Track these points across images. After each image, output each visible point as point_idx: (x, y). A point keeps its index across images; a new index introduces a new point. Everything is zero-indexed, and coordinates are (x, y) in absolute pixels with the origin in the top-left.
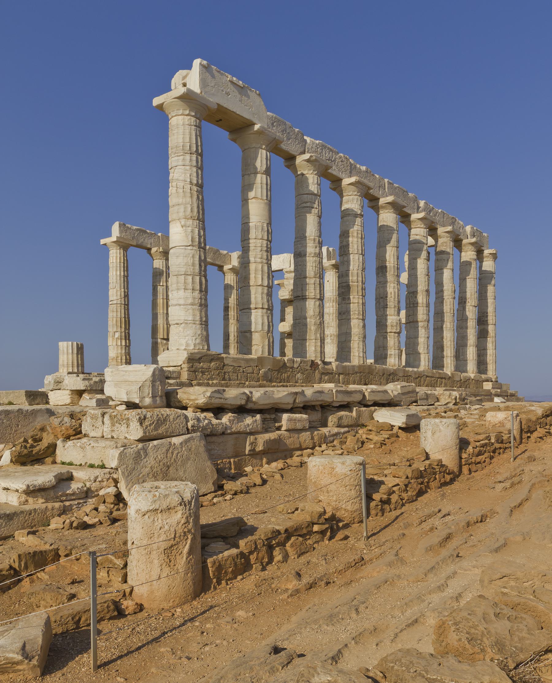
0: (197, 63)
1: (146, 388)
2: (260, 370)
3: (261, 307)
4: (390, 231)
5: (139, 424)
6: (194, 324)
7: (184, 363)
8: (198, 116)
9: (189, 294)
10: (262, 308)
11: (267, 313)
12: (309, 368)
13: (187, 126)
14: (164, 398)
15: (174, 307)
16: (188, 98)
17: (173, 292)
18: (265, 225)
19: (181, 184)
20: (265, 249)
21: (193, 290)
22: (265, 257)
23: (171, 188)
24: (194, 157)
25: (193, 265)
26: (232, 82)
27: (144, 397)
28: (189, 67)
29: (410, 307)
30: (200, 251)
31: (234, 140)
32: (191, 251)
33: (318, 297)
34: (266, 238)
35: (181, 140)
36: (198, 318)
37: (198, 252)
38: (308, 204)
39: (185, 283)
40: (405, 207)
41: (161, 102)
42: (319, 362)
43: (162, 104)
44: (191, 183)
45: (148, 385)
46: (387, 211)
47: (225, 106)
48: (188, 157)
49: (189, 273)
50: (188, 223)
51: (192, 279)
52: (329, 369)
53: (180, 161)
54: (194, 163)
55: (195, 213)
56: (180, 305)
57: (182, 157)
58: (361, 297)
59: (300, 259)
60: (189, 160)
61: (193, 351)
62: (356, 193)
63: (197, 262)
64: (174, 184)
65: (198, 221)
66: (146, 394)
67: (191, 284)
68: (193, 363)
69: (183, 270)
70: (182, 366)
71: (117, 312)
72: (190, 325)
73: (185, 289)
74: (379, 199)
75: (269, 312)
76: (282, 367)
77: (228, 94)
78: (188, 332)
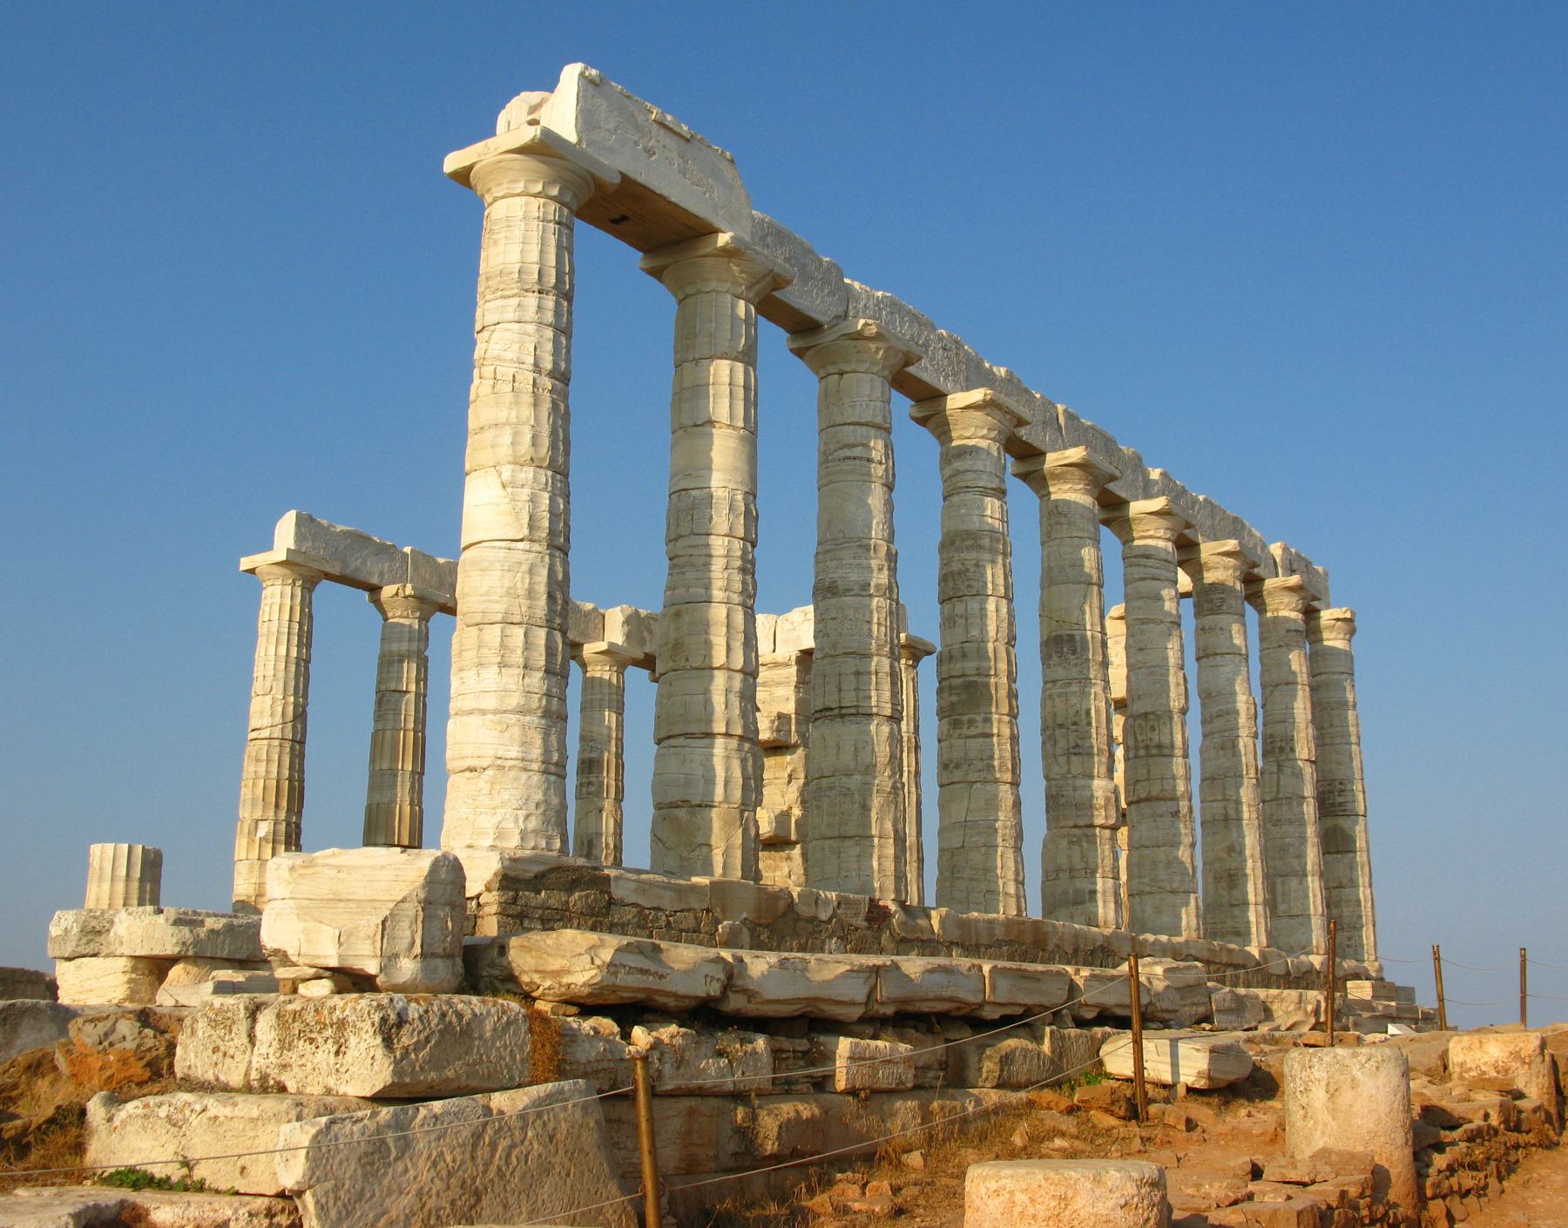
0: (571, 74)
1: (405, 924)
2: (717, 922)
3: (723, 730)
4: (1077, 541)
5: (379, 1040)
6: (525, 770)
7: (488, 889)
8: (568, 199)
9: (512, 678)
10: (727, 735)
11: (739, 749)
12: (860, 922)
13: (535, 222)
14: (459, 961)
15: (465, 719)
16: (544, 148)
17: (464, 674)
18: (740, 497)
19: (506, 371)
20: (738, 563)
21: (525, 667)
22: (738, 586)
23: (476, 381)
24: (550, 302)
25: (531, 594)
26: (662, 124)
27: (396, 956)
28: (550, 84)
29: (1137, 757)
30: (551, 556)
31: (656, 273)
32: (527, 556)
33: (888, 712)
34: (741, 532)
35: (516, 257)
36: (536, 752)
37: (547, 559)
38: (858, 451)
39: (503, 645)
40: (1113, 478)
41: (467, 164)
42: (893, 907)
43: (470, 168)
44: (537, 367)
45: (411, 913)
46: (1068, 486)
47: (641, 179)
48: (532, 300)
49: (517, 619)
50: (523, 475)
51: (526, 635)
52: (922, 930)
54: (549, 317)
55: (544, 449)
56: (483, 712)
57: (515, 301)
58: (1007, 718)
59: (833, 601)
60: (534, 308)
61: (519, 854)
62: (985, 432)
63: (542, 589)
64: (488, 371)
65: (550, 473)
66: (403, 944)
67: (519, 652)
68: (517, 892)
69: (497, 609)
70: (482, 900)
72: (512, 774)
73: (503, 665)
74: (1043, 454)
75: (747, 746)
76: (785, 914)
77: (650, 152)
78: (506, 796)
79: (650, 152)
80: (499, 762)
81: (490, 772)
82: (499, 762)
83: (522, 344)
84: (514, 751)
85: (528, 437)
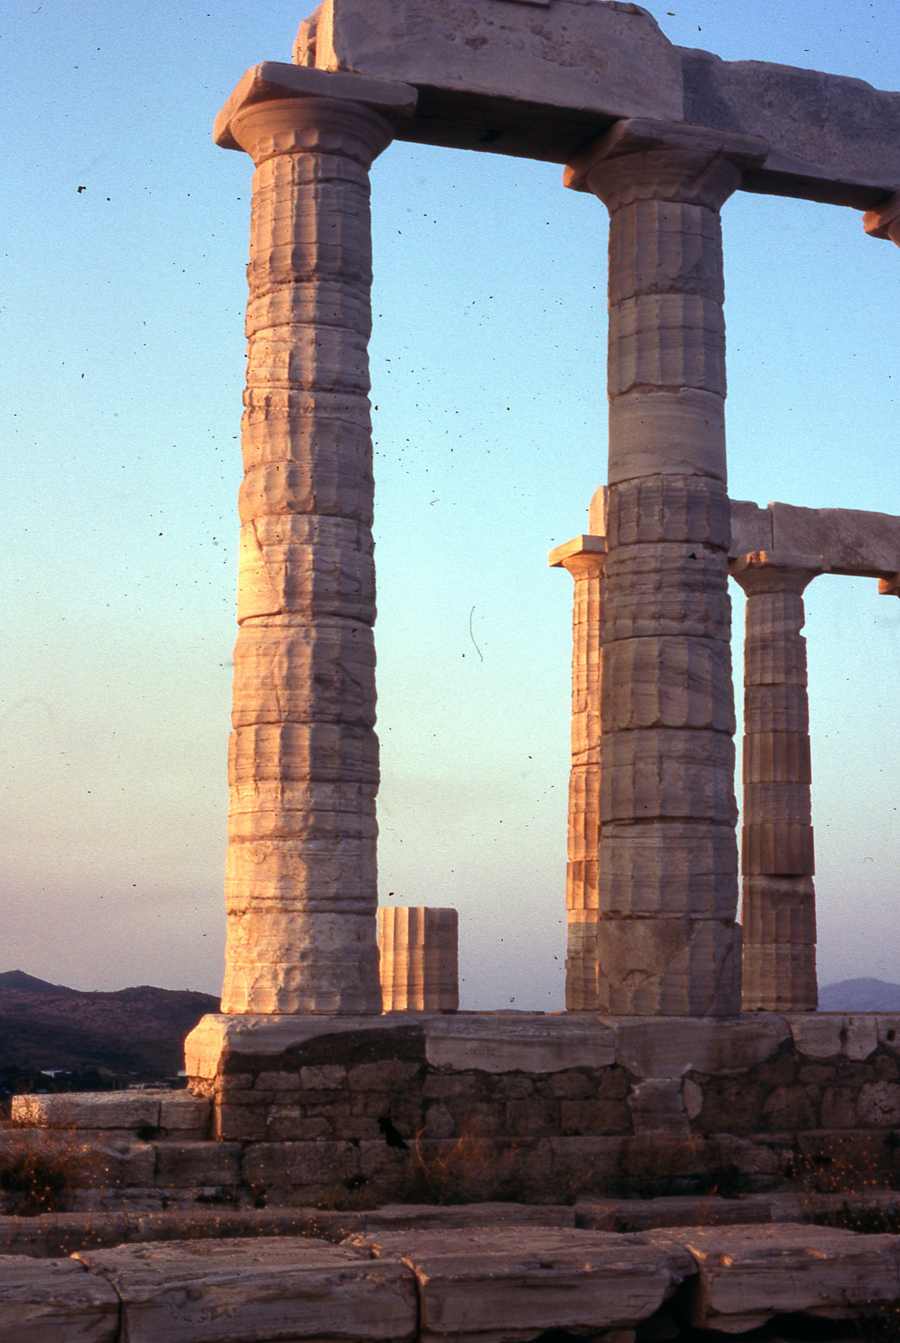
6: (285, 911)
24: (310, 291)
25: (291, 681)
32: (284, 633)
39: (258, 753)
44: (295, 381)
50: (279, 529)
51: (282, 737)
53: (264, 311)
54: (310, 310)
57: (266, 300)
67: (276, 759)
68: (256, 1075)
71: (588, 790)
72: (269, 918)
73: (259, 777)
79: (476, 43)
80: (254, 903)
81: (247, 917)
82: (254, 903)
83: (277, 352)
84: (271, 889)
85: (282, 478)
